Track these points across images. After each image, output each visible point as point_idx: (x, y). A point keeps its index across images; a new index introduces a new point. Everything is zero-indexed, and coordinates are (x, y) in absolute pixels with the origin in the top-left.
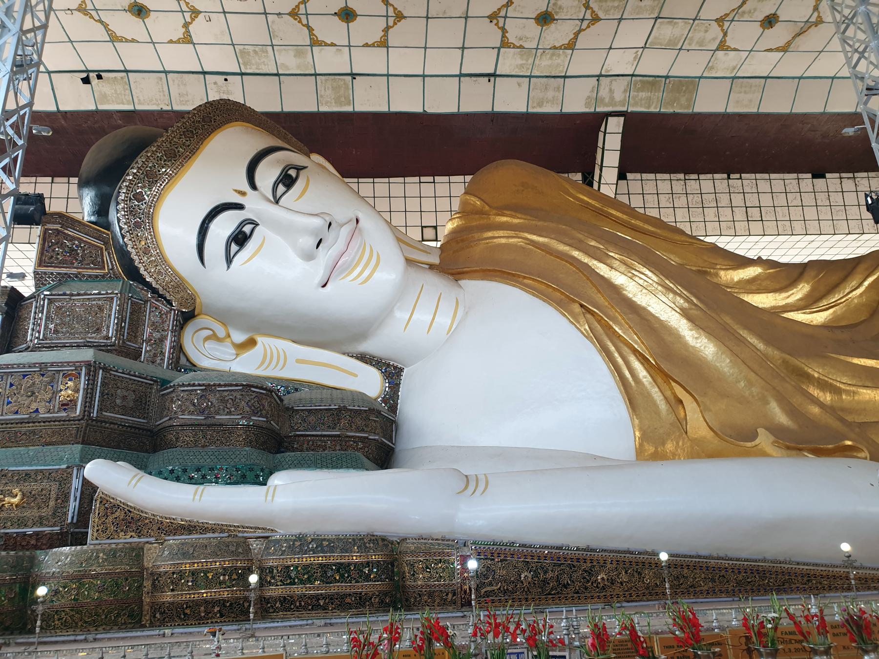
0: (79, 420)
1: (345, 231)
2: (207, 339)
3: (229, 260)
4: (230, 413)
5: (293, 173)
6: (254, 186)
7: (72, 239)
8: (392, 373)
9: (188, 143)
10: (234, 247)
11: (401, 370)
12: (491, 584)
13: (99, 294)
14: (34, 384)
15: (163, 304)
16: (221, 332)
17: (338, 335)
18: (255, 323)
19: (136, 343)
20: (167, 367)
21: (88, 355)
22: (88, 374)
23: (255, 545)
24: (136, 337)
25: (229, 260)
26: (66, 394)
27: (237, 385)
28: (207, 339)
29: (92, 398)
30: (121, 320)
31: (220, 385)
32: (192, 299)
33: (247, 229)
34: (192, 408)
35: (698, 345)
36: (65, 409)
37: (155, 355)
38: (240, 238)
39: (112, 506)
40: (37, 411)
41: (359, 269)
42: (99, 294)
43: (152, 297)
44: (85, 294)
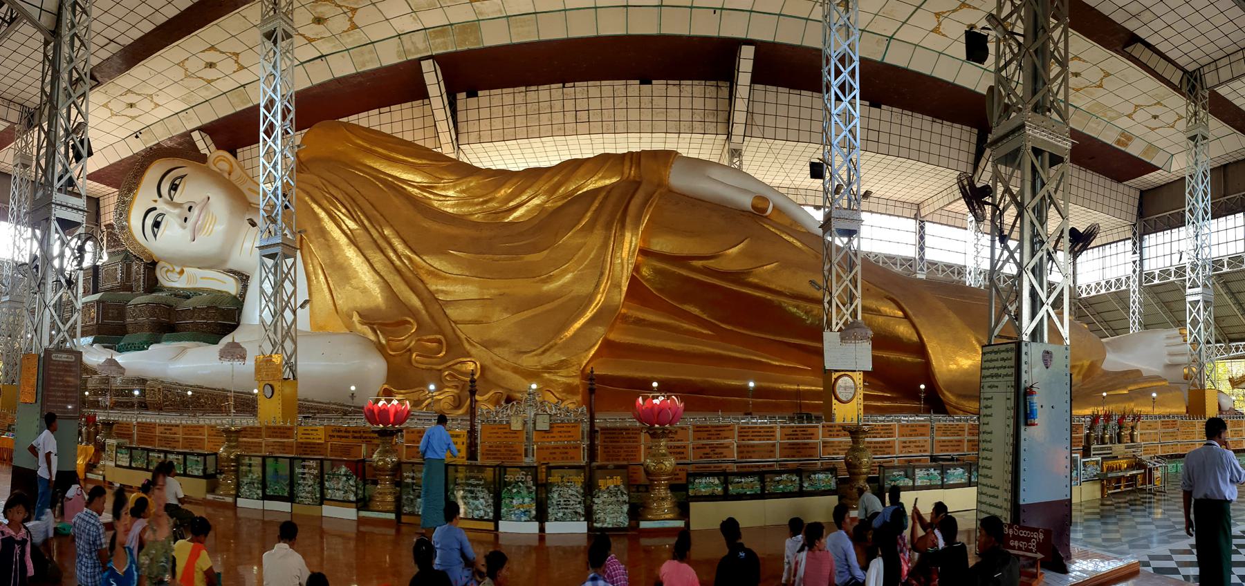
6: (160, 196)
18: (184, 262)
38: (157, 224)
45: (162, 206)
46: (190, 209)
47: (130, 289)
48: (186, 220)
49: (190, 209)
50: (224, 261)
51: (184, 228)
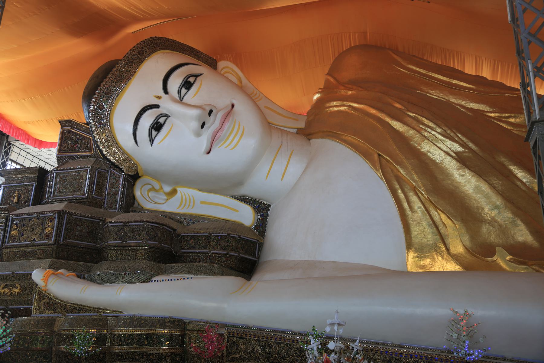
0: (53, 245)
1: (220, 116)
2: (149, 190)
3: (152, 141)
4: (136, 239)
5: (191, 80)
6: (166, 91)
7: (77, 134)
8: (262, 209)
9: (129, 69)
10: (154, 133)
11: (269, 206)
12: (235, 353)
13: (81, 168)
14: (34, 224)
15: (117, 171)
16: (157, 187)
17: (225, 184)
18: (176, 179)
19: (101, 196)
20: (118, 211)
21: (60, 206)
22: (59, 218)
23: (111, 321)
24: (101, 192)
25: (152, 141)
26: (48, 230)
27: (140, 222)
28: (149, 190)
29: (61, 232)
30: (91, 183)
31: (131, 222)
32: (134, 167)
33: (162, 120)
34: (116, 236)
35: (463, 181)
36: (47, 239)
37: (112, 203)
38: (157, 127)
39: (43, 296)
40: (34, 240)
41: (229, 141)
42: (81, 168)
43: (112, 167)
44: (74, 169)
45: (167, 105)
46: (211, 112)
47: (100, 205)
48: (203, 126)
49: (211, 112)
50: (240, 184)
51: (198, 135)
